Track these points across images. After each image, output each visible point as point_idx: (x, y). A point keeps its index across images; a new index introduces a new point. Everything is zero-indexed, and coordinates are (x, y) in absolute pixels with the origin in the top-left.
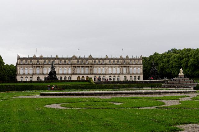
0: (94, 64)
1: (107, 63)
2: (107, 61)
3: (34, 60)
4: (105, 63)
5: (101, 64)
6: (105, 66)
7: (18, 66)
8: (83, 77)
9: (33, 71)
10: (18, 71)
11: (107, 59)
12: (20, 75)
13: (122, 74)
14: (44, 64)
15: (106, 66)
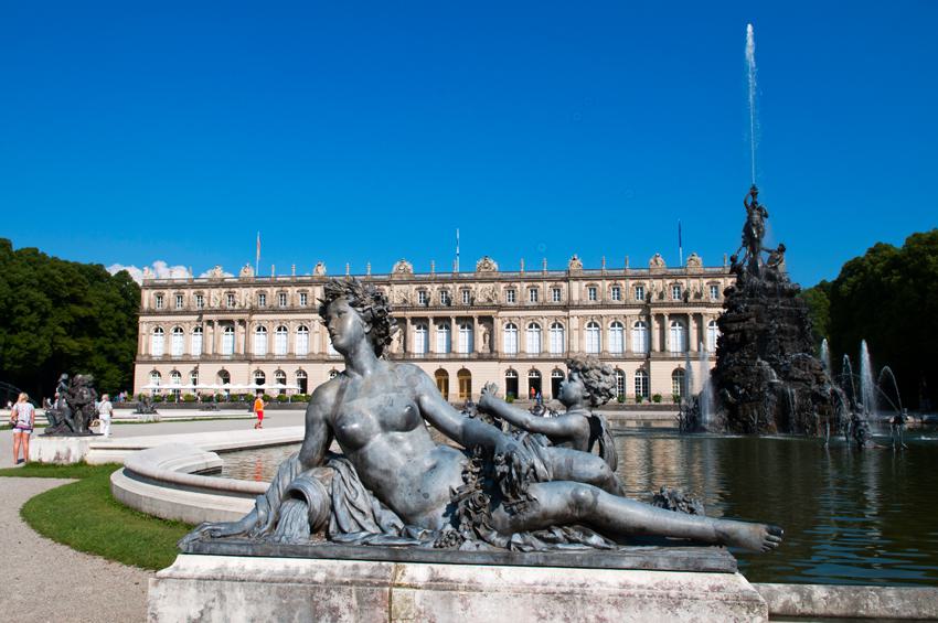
0: (500, 308)
1: (576, 297)
2: (575, 285)
3: (214, 292)
4: (564, 298)
5: (539, 308)
6: (560, 313)
7: (141, 319)
8: (441, 373)
9: (204, 344)
10: (143, 340)
11: (576, 279)
12: (150, 361)
13: (663, 354)
14: (253, 311)
15: (572, 312)
